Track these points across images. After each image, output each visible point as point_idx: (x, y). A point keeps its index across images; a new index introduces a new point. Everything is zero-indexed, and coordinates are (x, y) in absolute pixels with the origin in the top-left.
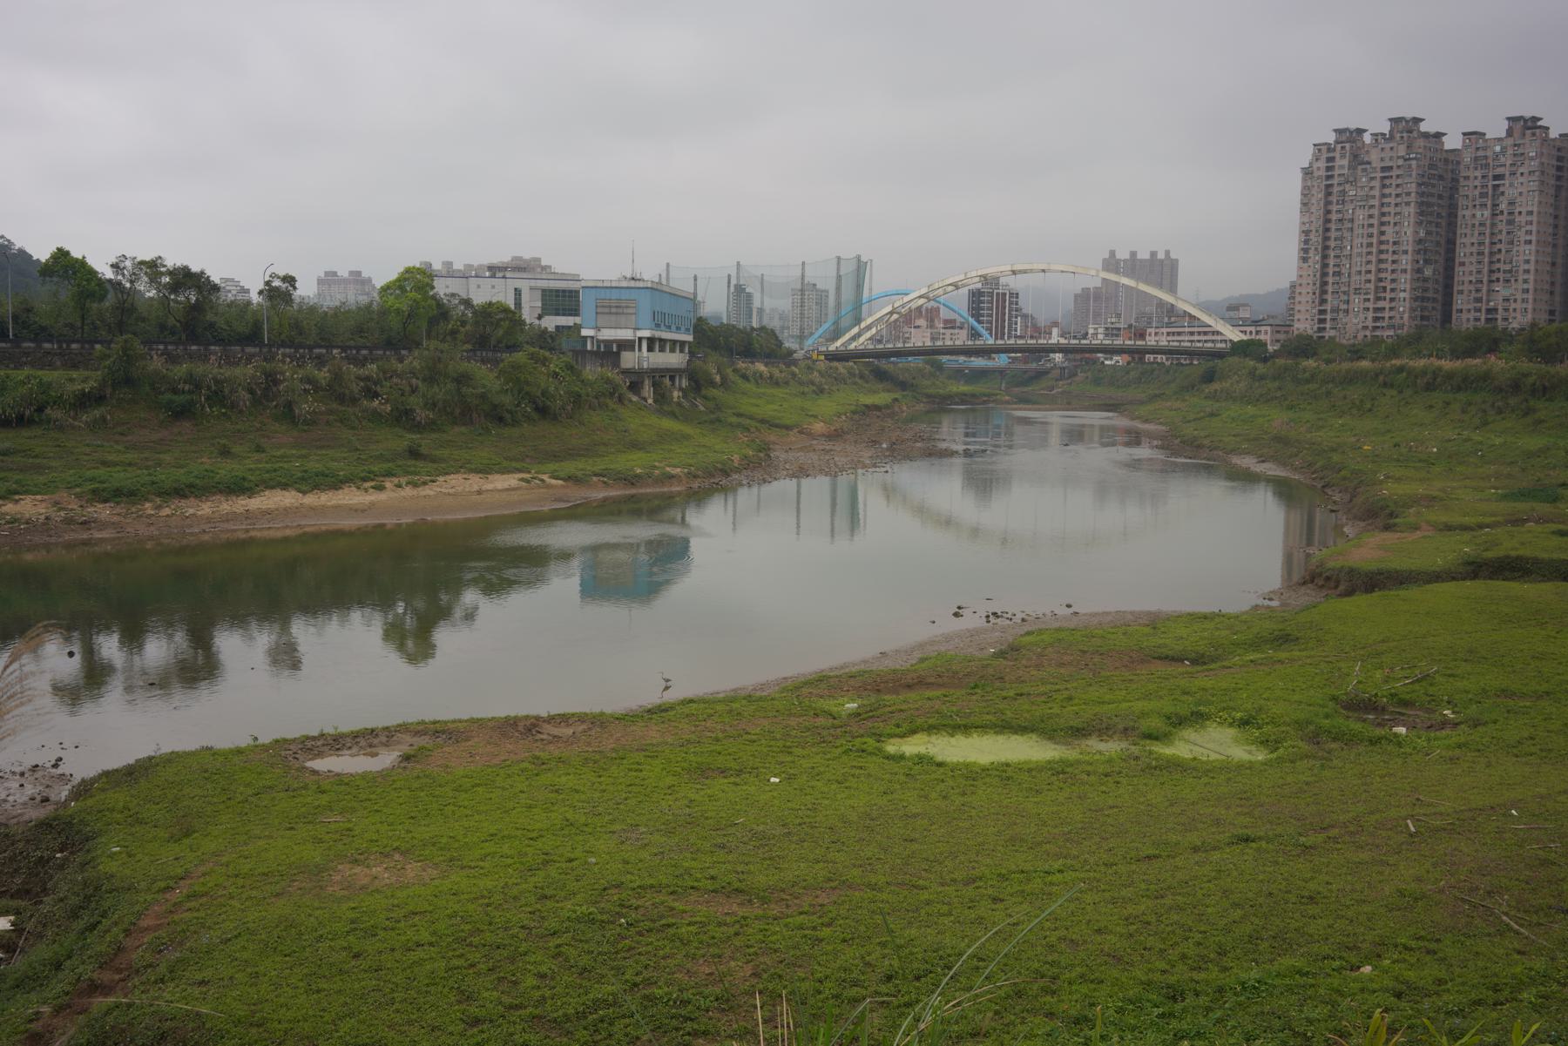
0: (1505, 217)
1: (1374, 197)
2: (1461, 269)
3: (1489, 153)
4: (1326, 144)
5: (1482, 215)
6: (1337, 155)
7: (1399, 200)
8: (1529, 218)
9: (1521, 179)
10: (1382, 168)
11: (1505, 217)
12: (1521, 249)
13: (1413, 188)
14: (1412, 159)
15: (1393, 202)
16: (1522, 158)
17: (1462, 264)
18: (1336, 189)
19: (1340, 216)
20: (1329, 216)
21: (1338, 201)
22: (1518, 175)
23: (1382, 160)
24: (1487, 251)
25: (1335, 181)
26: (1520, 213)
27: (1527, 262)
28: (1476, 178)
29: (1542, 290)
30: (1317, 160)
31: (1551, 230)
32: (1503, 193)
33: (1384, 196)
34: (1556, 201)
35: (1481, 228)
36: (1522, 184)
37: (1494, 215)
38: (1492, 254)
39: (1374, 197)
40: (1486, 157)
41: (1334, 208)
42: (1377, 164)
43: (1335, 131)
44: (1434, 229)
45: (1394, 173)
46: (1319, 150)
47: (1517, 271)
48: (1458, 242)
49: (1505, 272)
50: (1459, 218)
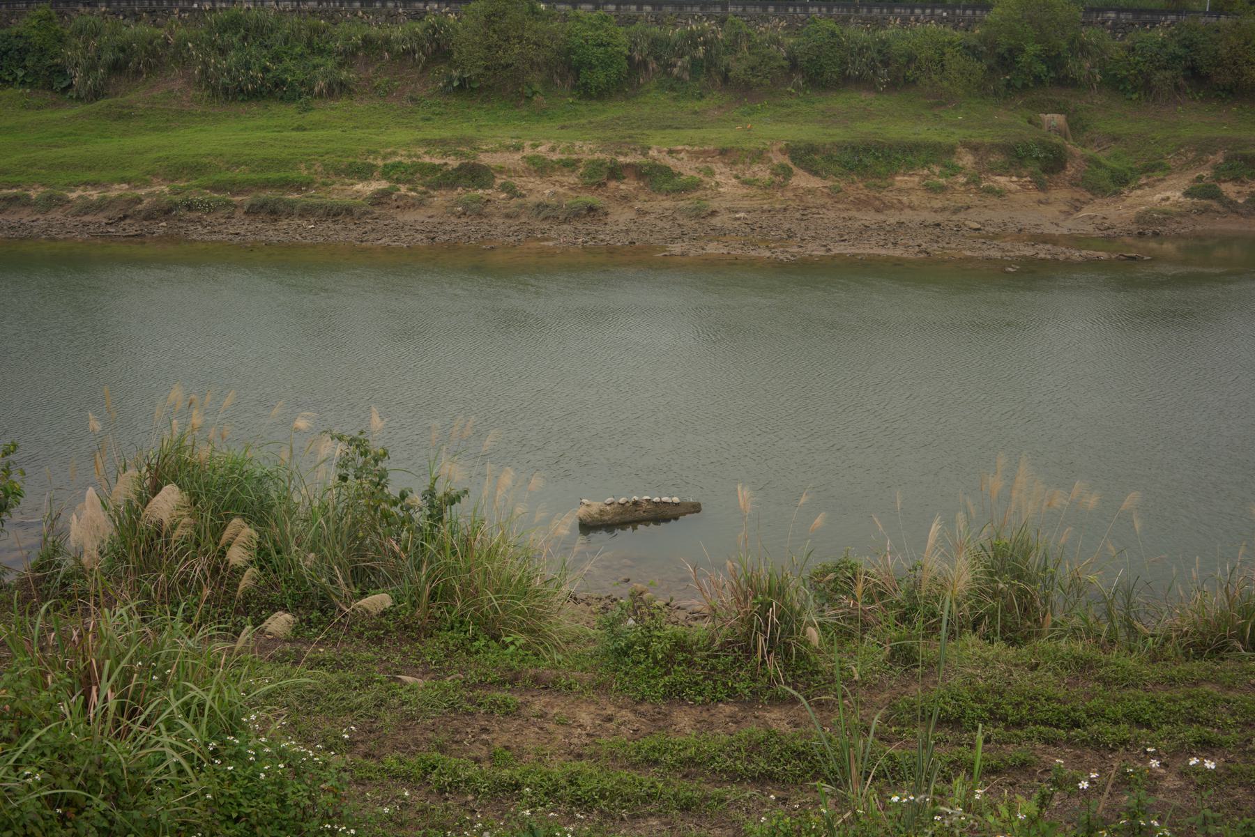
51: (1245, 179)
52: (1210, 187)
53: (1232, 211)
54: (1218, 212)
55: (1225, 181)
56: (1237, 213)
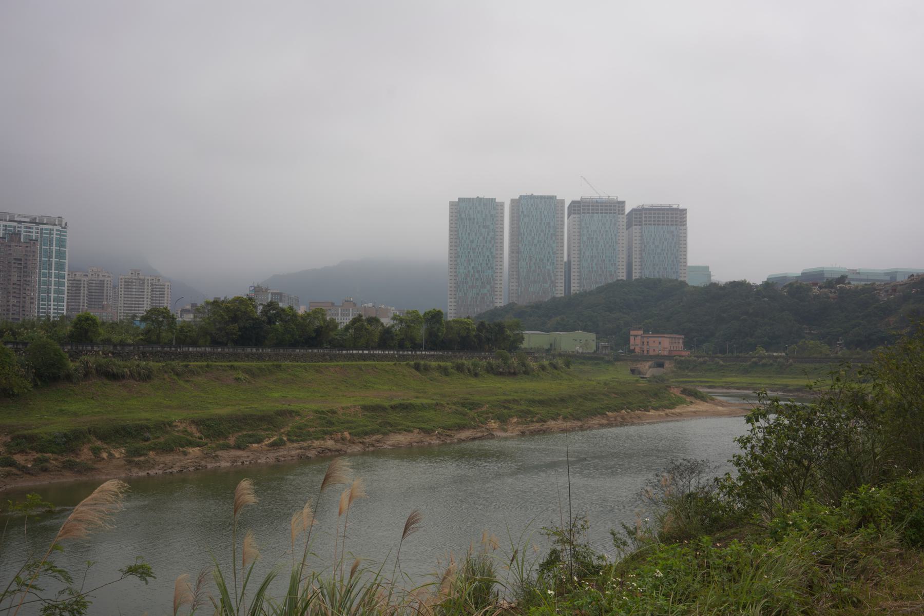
51: (28, 451)
52: (7, 459)
53: (26, 473)
54: (17, 475)
55: (15, 454)
56: (29, 473)
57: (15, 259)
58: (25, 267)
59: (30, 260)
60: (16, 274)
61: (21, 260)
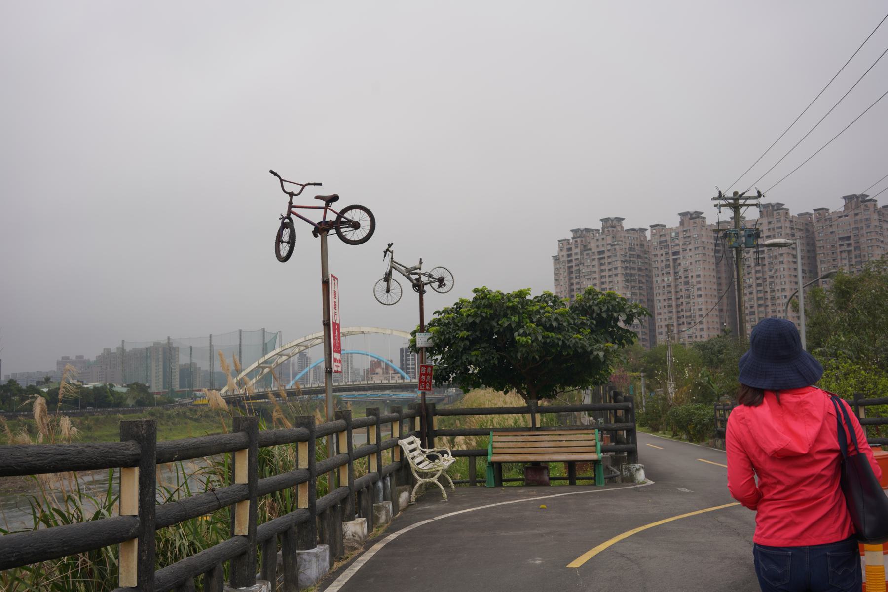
0: (683, 280)
1: (595, 272)
2: (659, 317)
3: (668, 238)
4: (565, 240)
5: (668, 280)
6: (573, 247)
7: (610, 273)
8: (698, 279)
9: (690, 254)
10: (598, 252)
11: (683, 280)
12: (695, 301)
13: (619, 264)
14: (617, 244)
15: (607, 275)
16: (689, 239)
17: (660, 314)
18: (575, 268)
19: (578, 286)
20: (572, 287)
21: (576, 277)
22: (688, 250)
23: (598, 247)
24: (674, 304)
25: (573, 264)
26: (692, 276)
27: (700, 309)
28: (662, 255)
29: (714, 328)
30: (561, 250)
31: (715, 287)
32: (680, 264)
33: (602, 271)
34: (717, 267)
35: (669, 289)
36: (691, 256)
37: (676, 279)
38: (677, 306)
39: (595, 272)
40: (666, 241)
41: (574, 281)
42: (595, 250)
43: (572, 231)
44: (638, 291)
45: (606, 255)
46: (563, 244)
47: (694, 317)
48: (655, 299)
49: (687, 317)
50: (655, 283)
57: (840, 238)
58: (858, 248)
59: (863, 235)
60: (846, 262)
61: (849, 238)
